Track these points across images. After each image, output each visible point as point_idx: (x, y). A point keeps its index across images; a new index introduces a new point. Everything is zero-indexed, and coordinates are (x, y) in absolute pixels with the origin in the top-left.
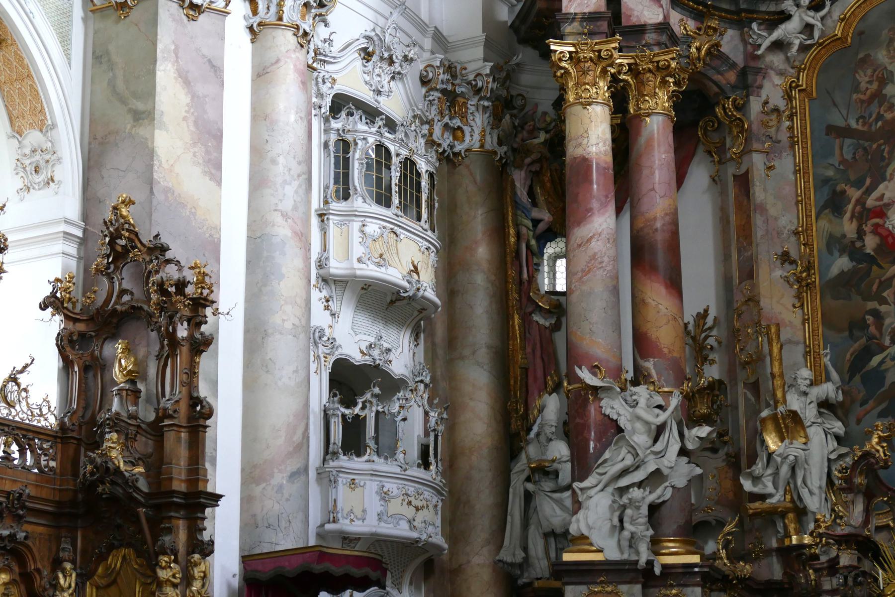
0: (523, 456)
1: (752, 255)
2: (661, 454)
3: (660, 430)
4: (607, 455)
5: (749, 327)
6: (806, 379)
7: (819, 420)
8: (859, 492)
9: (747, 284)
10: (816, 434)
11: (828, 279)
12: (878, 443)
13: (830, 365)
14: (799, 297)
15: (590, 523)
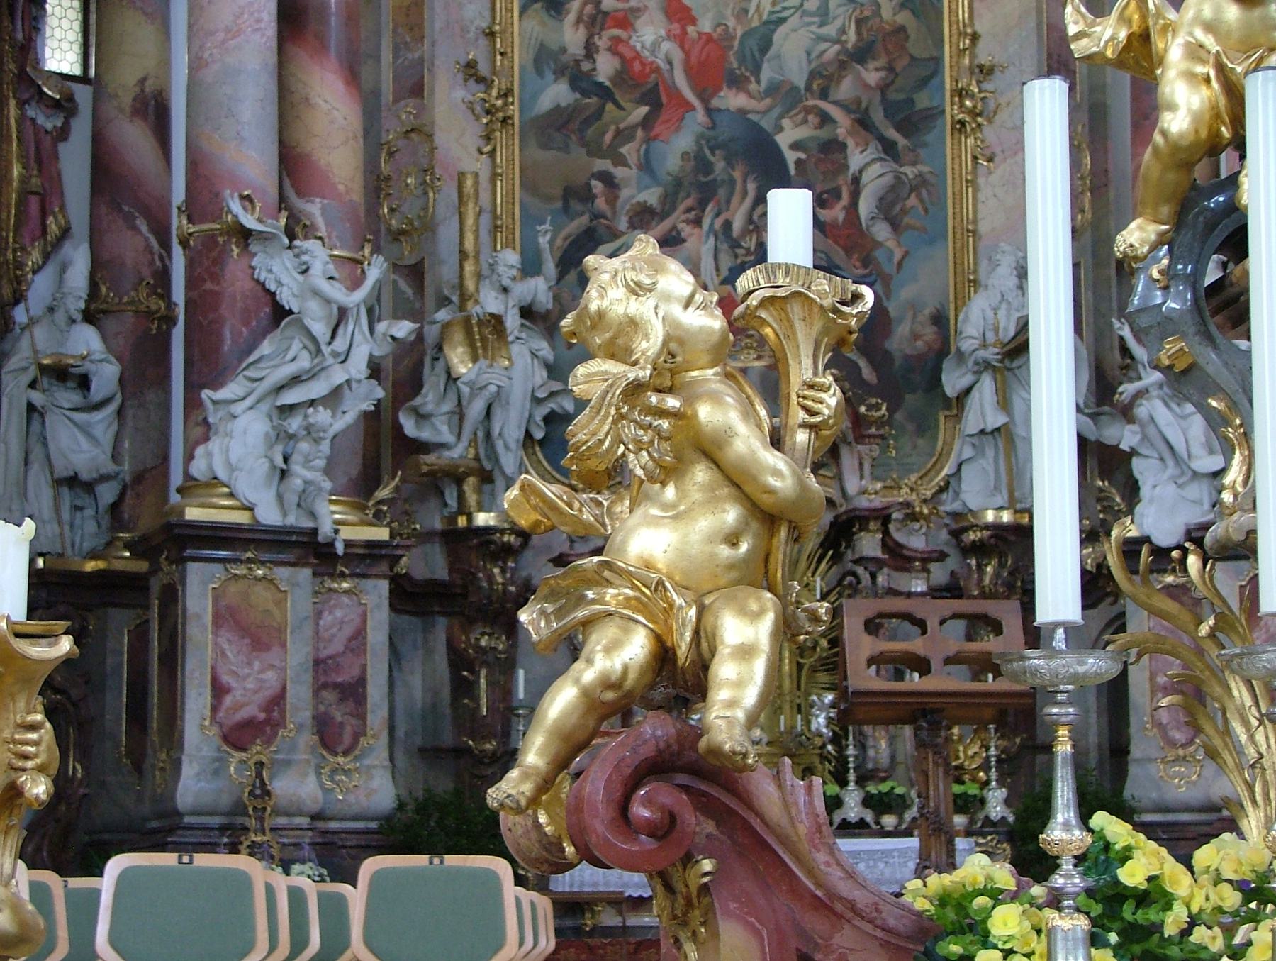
0: (25, 343)
1: (421, 60)
4: (266, 348)
5: (408, 175)
6: (512, 266)
7: (524, 335)
9: (410, 105)
11: (533, 115)
13: (548, 250)
14: (488, 138)
15: (233, 459)
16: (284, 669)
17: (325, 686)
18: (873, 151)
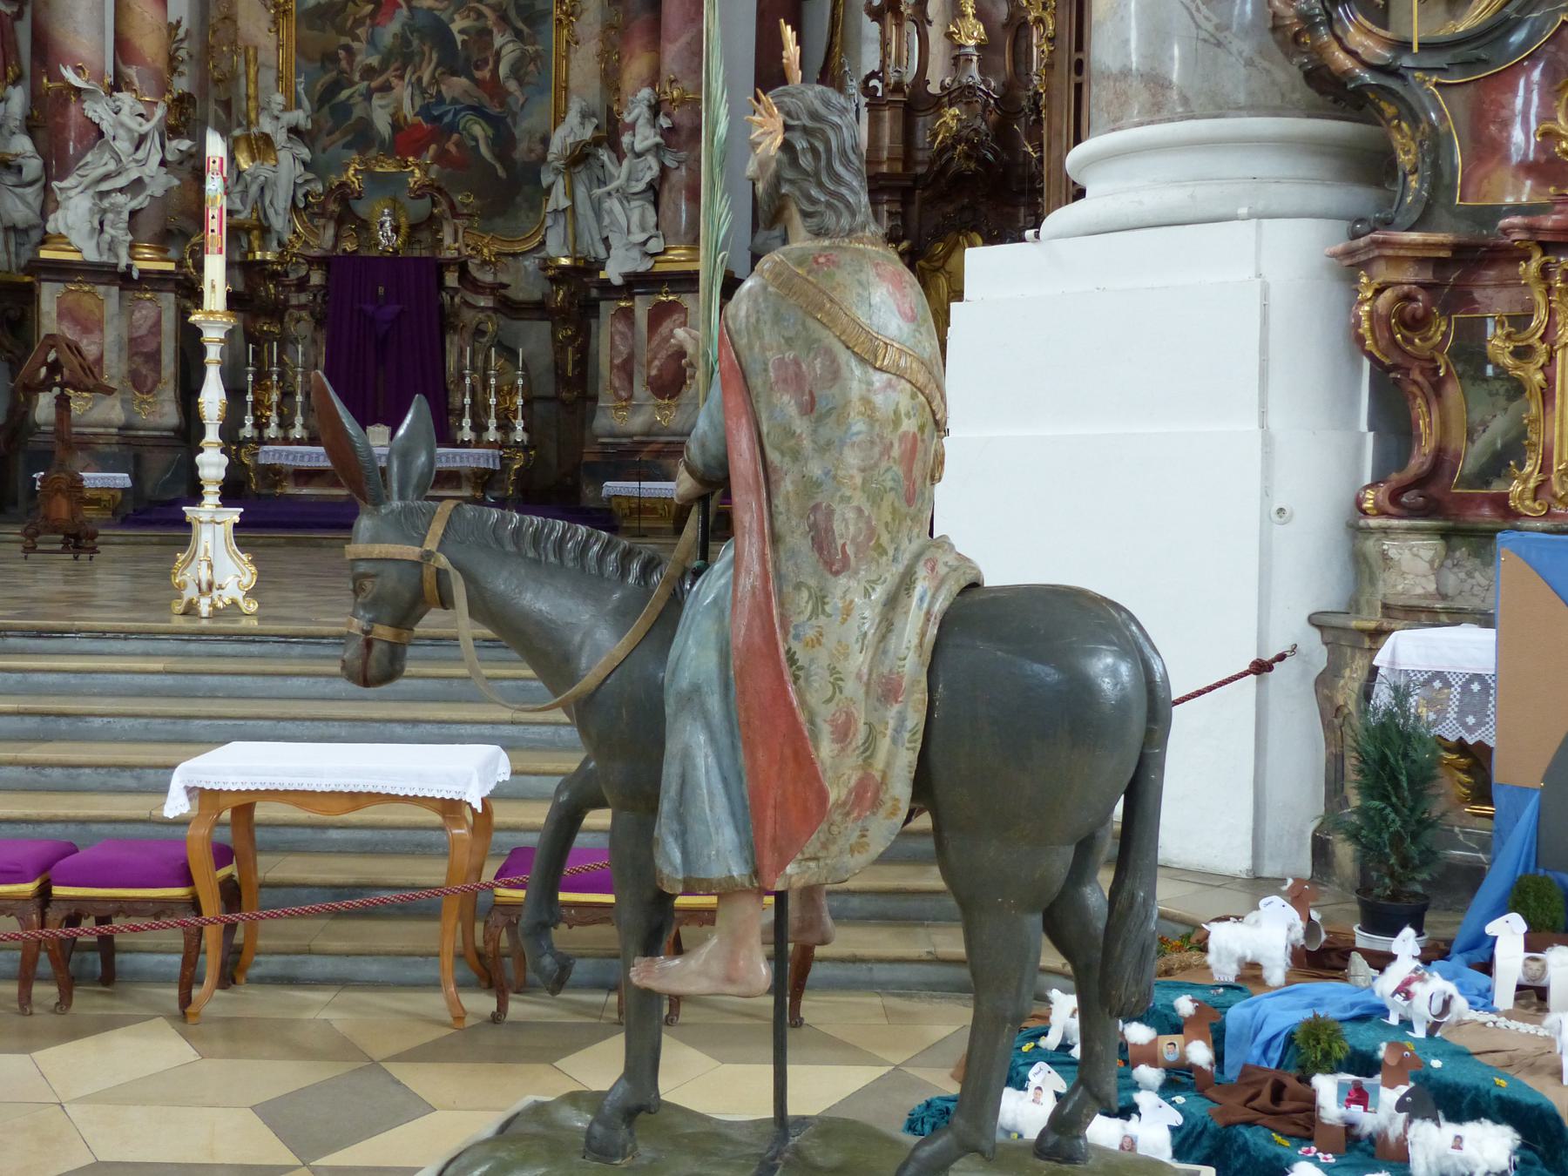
2: (142, 163)
3: (141, 140)
4: (89, 157)
8: (331, 218)
10: (285, 157)
12: (354, 175)
14: (275, 22)
16: (102, 344)
17: (136, 354)
18: (508, 37)
